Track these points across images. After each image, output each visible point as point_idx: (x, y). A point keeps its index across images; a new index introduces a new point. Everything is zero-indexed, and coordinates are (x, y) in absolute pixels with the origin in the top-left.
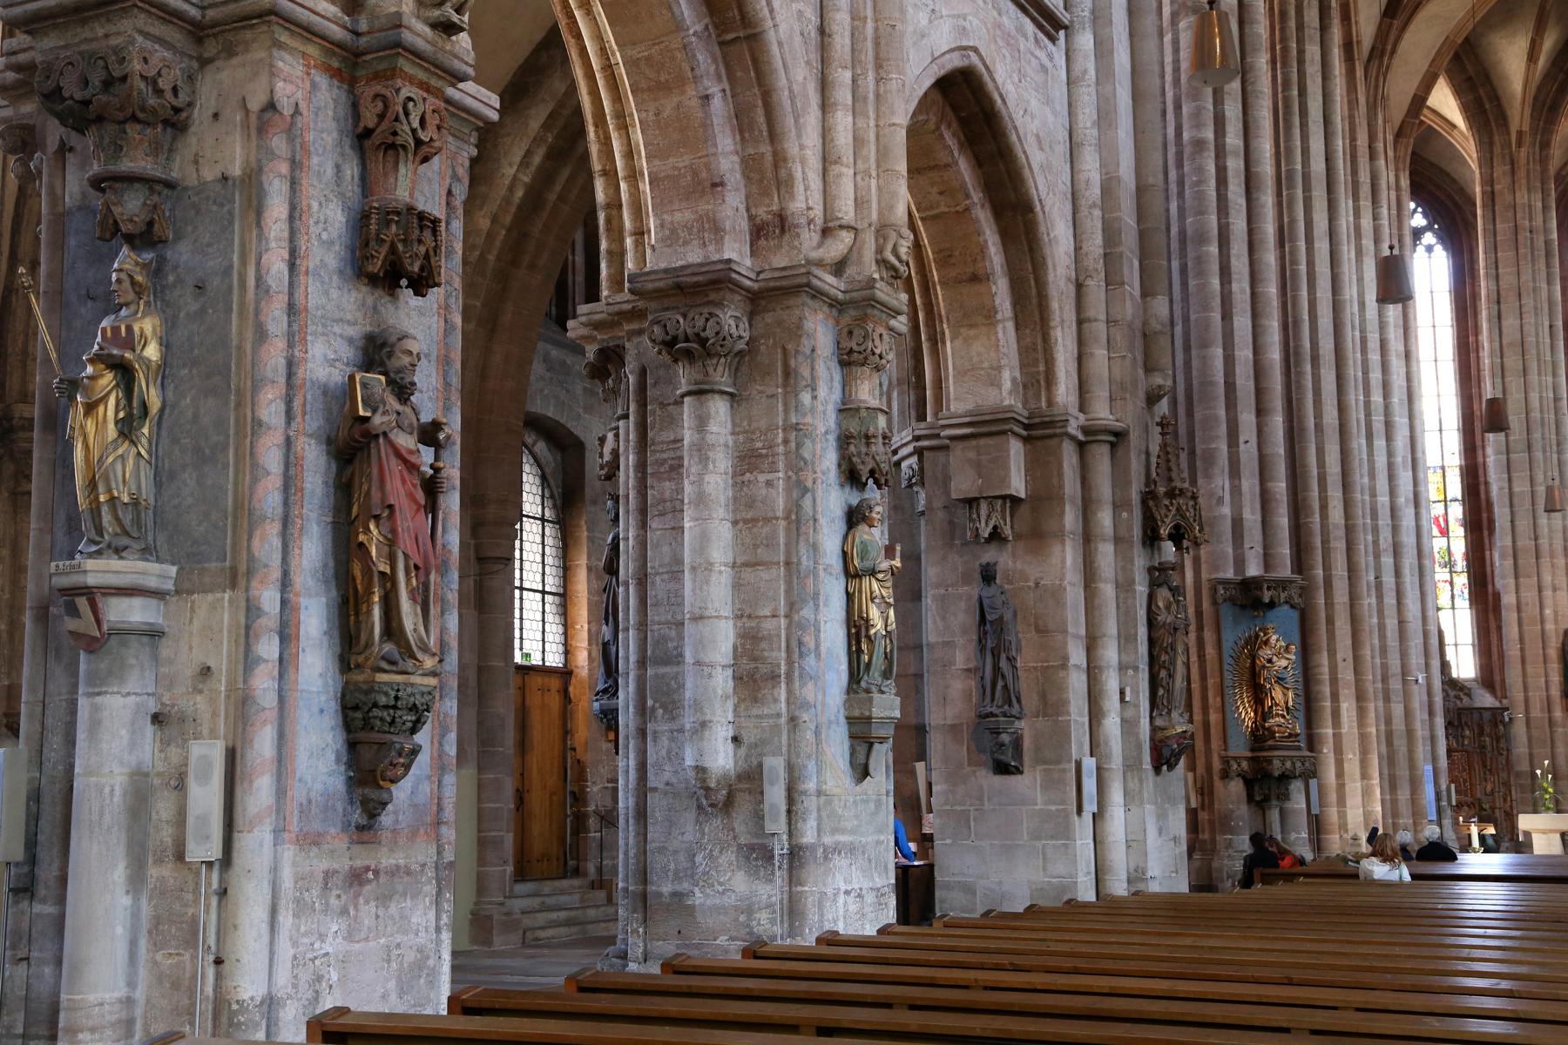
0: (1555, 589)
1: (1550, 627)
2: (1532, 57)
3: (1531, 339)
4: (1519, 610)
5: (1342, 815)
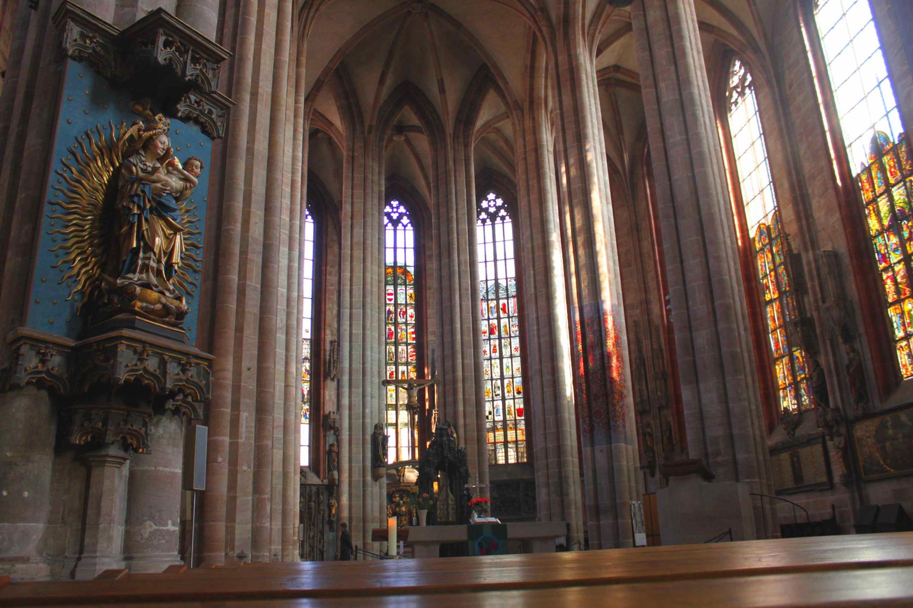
0: (372, 397)
1: (368, 420)
2: (382, 82)
3: (369, 242)
5: (230, 531)
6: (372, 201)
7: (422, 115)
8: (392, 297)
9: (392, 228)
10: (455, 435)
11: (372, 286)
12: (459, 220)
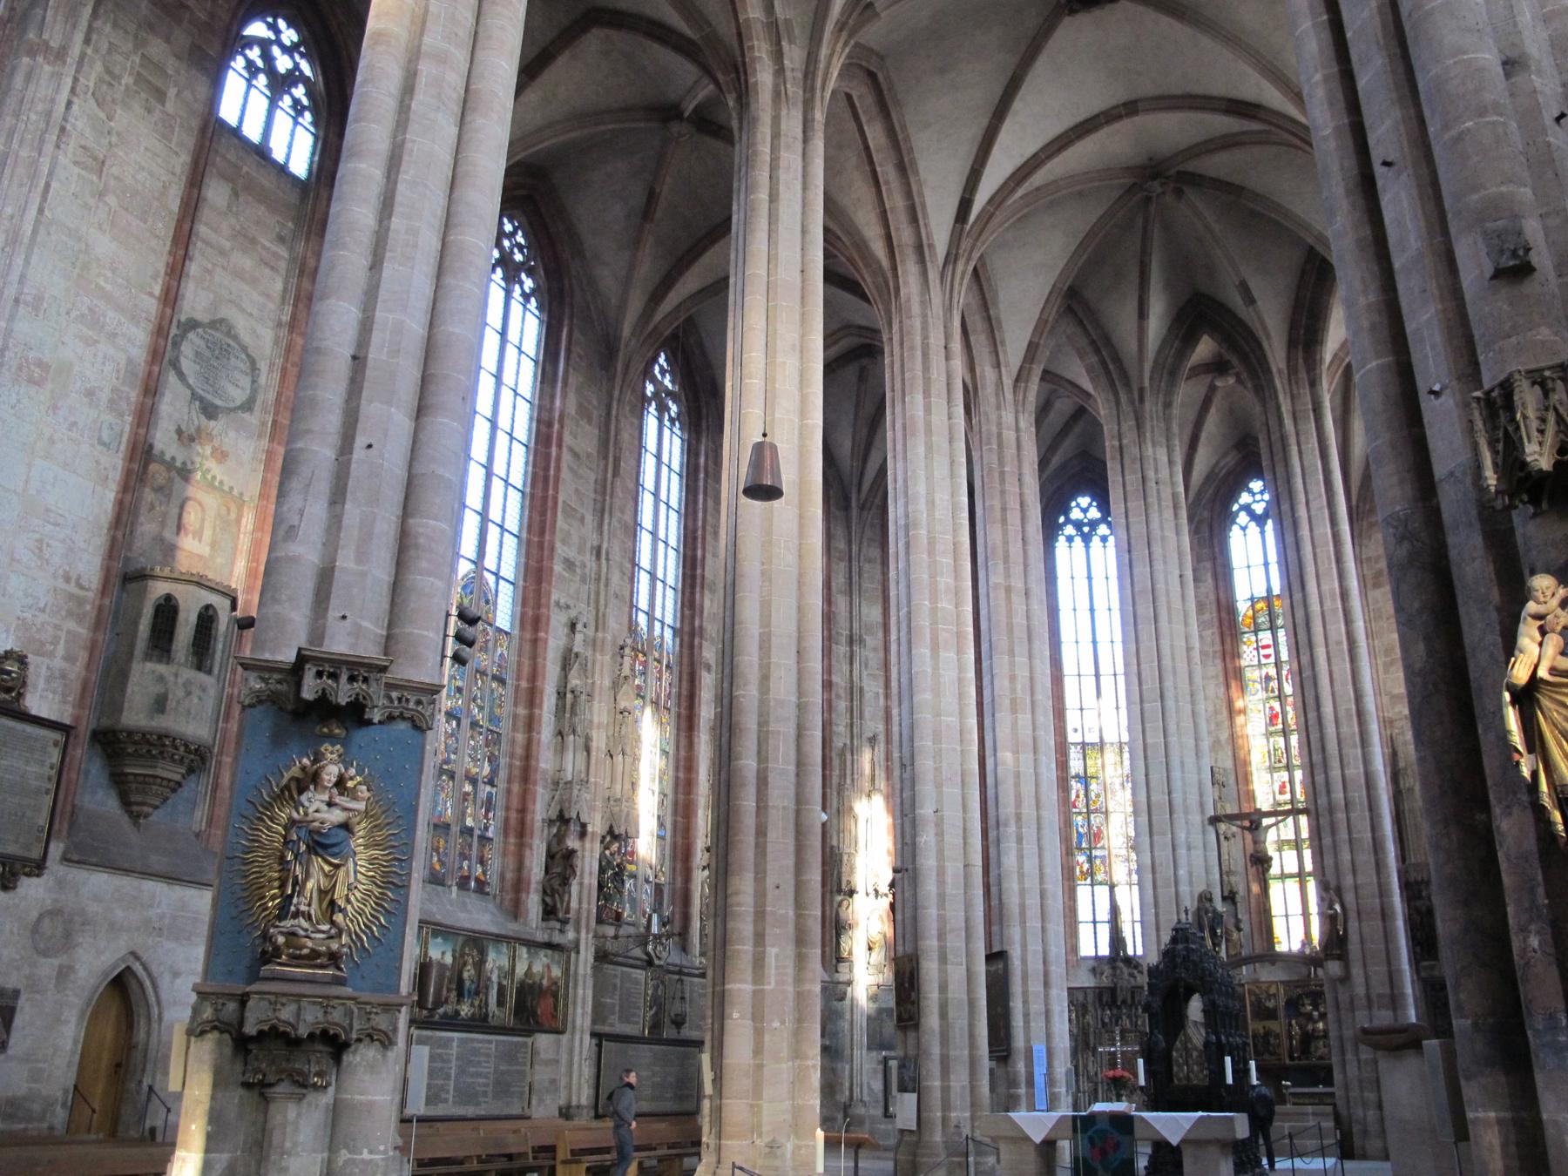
0: (1189, 848)
3: (1160, 586)
4: (1154, 871)
6: (1161, 515)
7: (1233, 346)
8: (1271, 651)
9: (1258, 529)
10: (1337, 907)
11: (1173, 659)
12: (1313, 521)
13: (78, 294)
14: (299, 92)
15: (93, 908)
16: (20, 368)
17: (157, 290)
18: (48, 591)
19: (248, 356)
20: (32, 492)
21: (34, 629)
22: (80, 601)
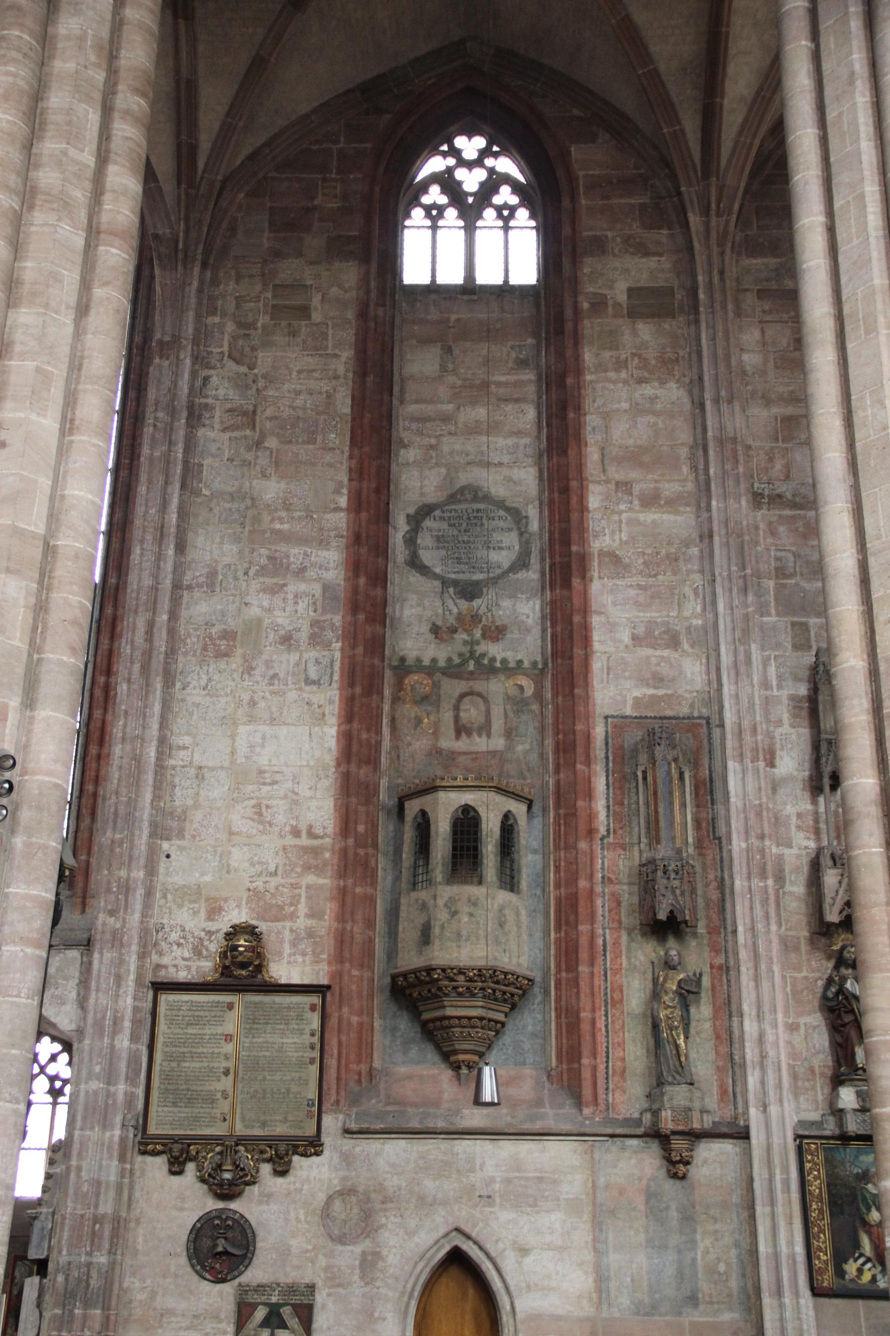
13: (253, 551)
14: (505, 195)
15: (393, 1182)
16: (205, 648)
17: (343, 501)
18: (277, 853)
19: (508, 509)
20: (240, 760)
21: (268, 896)
22: (315, 851)
